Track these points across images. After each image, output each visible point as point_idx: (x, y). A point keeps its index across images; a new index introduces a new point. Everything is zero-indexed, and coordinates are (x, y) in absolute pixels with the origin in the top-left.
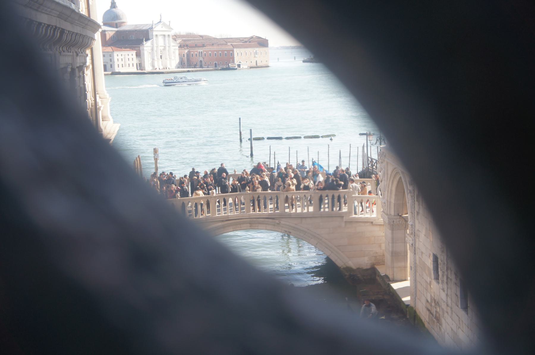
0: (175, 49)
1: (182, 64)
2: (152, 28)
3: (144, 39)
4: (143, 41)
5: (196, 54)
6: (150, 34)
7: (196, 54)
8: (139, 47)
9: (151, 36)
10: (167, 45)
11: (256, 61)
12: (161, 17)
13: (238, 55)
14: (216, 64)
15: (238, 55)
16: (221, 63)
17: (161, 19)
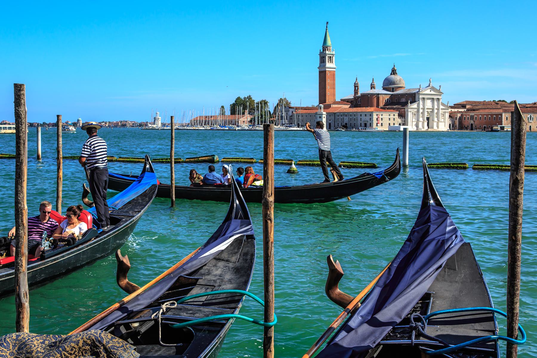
0: (445, 112)
1: (452, 126)
2: (419, 91)
3: (409, 101)
4: (408, 103)
5: (468, 117)
6: (417, 97)
7: (468, 117)
8: (405, 108)
9: (418, 99)
10: (436, 107)
11: (530, 126)
12: (430, 82)
13: (507, 119)
14: (485, 127)
15: (507, 119)
16: (489, 127)
17: (430, 84)
